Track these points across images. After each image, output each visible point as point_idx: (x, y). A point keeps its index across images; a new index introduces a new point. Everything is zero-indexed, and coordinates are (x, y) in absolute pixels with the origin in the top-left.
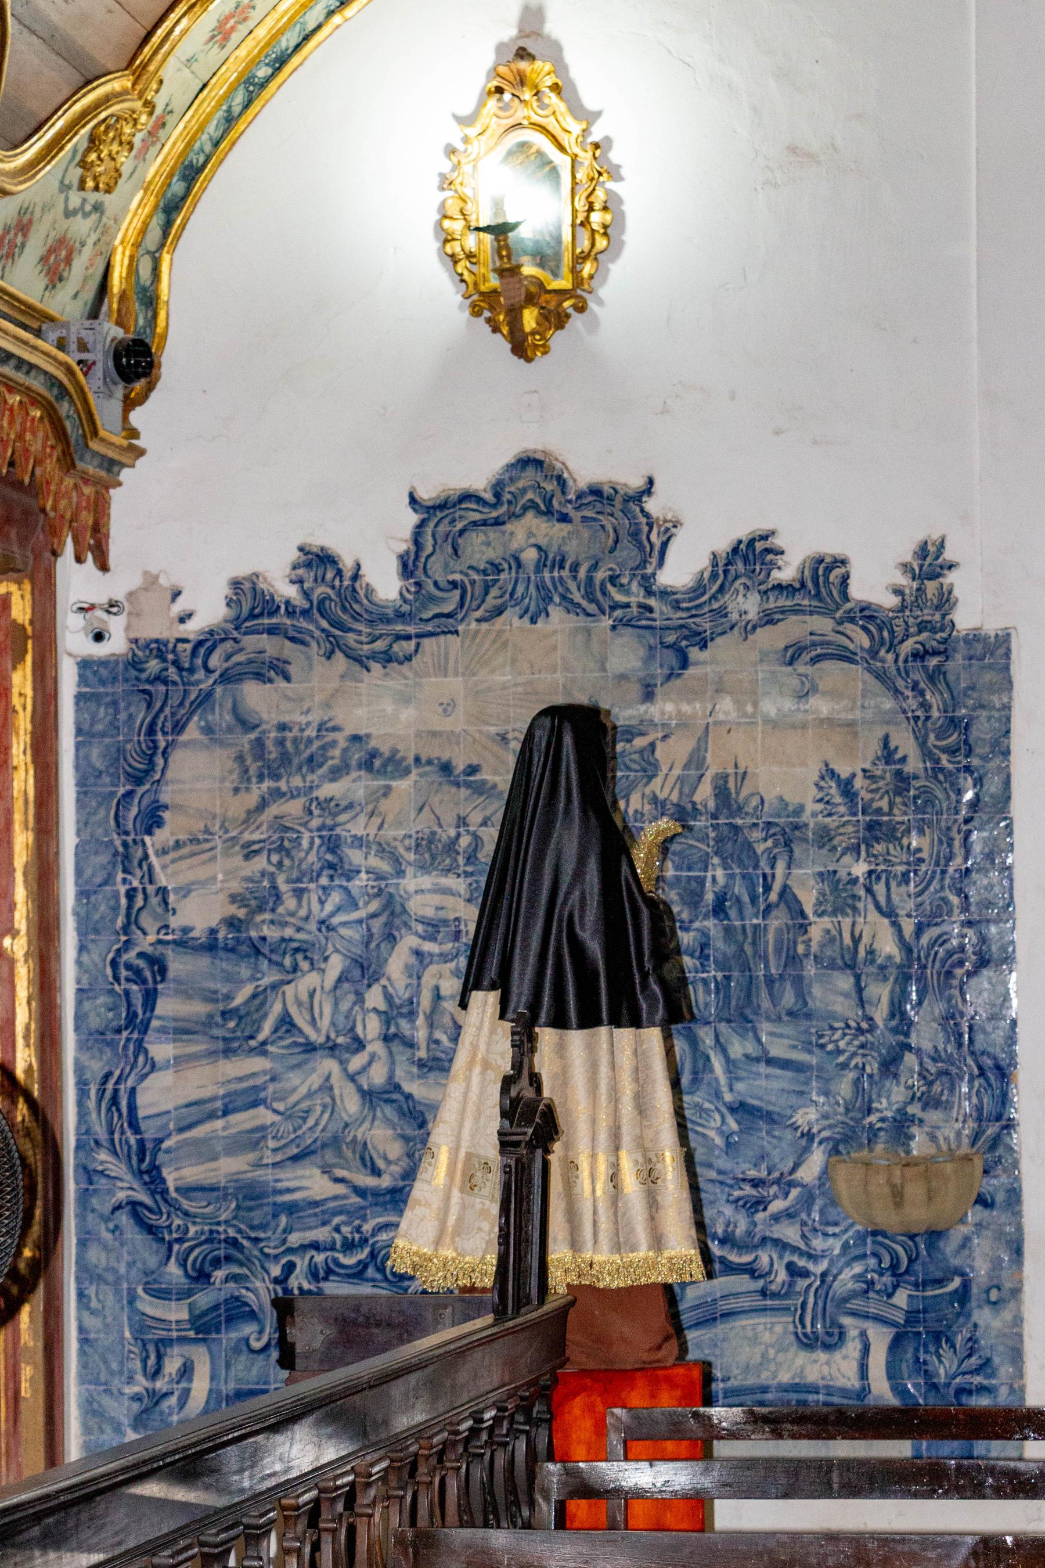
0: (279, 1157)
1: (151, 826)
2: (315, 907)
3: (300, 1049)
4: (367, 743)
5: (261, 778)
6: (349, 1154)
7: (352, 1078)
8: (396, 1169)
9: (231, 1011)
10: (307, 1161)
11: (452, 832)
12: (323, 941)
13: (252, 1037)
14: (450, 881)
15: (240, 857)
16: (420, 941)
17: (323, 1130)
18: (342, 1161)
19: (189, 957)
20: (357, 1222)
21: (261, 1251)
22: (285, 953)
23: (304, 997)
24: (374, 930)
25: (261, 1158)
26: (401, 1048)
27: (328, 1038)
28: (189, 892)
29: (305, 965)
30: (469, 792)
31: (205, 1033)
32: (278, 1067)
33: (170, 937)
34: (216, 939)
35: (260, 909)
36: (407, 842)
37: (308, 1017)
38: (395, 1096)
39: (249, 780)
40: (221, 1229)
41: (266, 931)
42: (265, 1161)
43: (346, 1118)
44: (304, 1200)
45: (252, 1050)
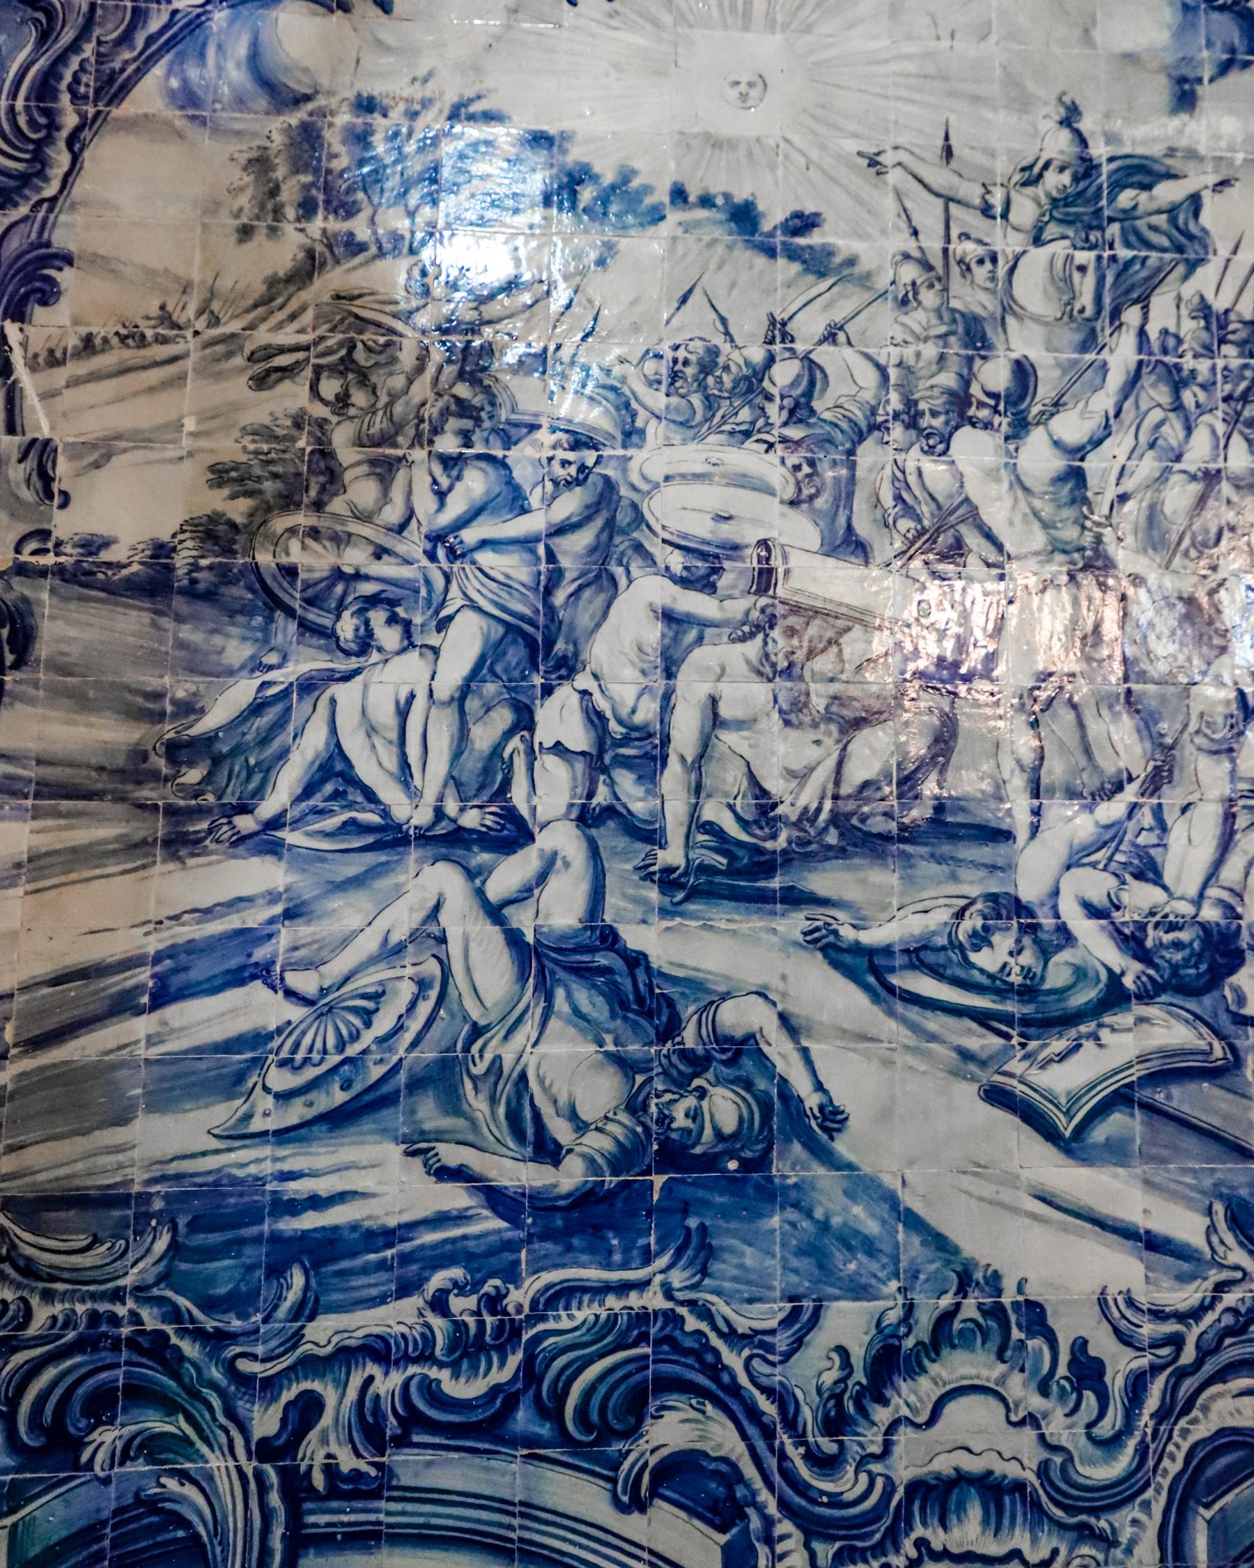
0: (296, 1113)
1: (26, 297)
2: (424, 503)
3: (370, 839)
4: (564, 152)
5: (307, 208)
6: (478, 1104)
7: (495, 912)
8: (597, 1143)
9: (193, 742)
10: (368, 1124)
11: (757, 354)
12: (439, 582)
13: (244, 809)
14: (749, 459)
15: (244, 379)
16: (676, 590)
17: (414, 1044)
18: (460, 1123)
19: (93, 608)
20: (490, 1286)
21: (230, 1367)
22: (341, 607)
23: (385, 715)
24: (565, 562)
25: (248, 1117)
26: (622, 842)
27: (439, 814)
28: (108, 457)
29: (389, 637)
30: (796, 267)
31: (121, 798)
32: (304, 884)
33: (49, 560)
34: (170, 569)
35: (288, 502)
36: (650, 366)
37: (391, 763)
38: (602, 959)
39: (278, 213)
40: (121, 1311)
41: (296, 554)
42: (257, 1125)
43: (475, 1014)
44: (354, 1227)
45: (241, 840)
